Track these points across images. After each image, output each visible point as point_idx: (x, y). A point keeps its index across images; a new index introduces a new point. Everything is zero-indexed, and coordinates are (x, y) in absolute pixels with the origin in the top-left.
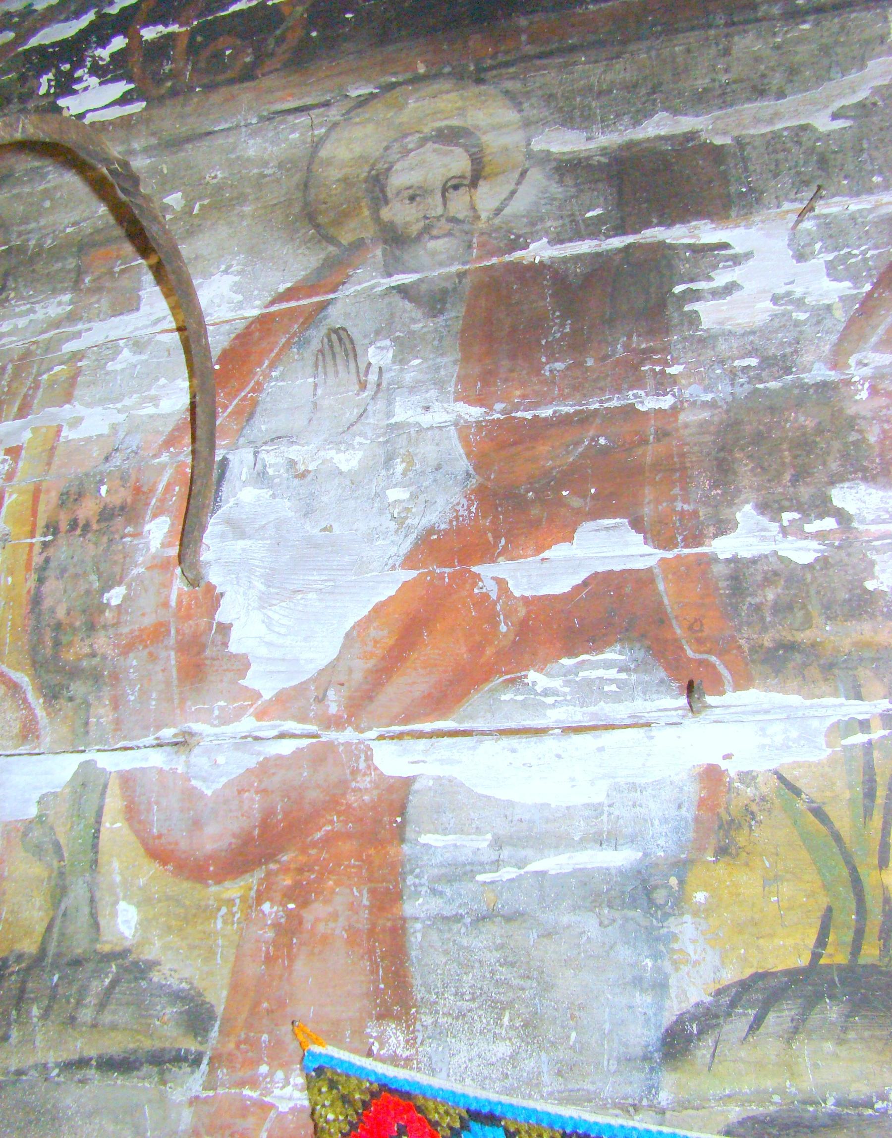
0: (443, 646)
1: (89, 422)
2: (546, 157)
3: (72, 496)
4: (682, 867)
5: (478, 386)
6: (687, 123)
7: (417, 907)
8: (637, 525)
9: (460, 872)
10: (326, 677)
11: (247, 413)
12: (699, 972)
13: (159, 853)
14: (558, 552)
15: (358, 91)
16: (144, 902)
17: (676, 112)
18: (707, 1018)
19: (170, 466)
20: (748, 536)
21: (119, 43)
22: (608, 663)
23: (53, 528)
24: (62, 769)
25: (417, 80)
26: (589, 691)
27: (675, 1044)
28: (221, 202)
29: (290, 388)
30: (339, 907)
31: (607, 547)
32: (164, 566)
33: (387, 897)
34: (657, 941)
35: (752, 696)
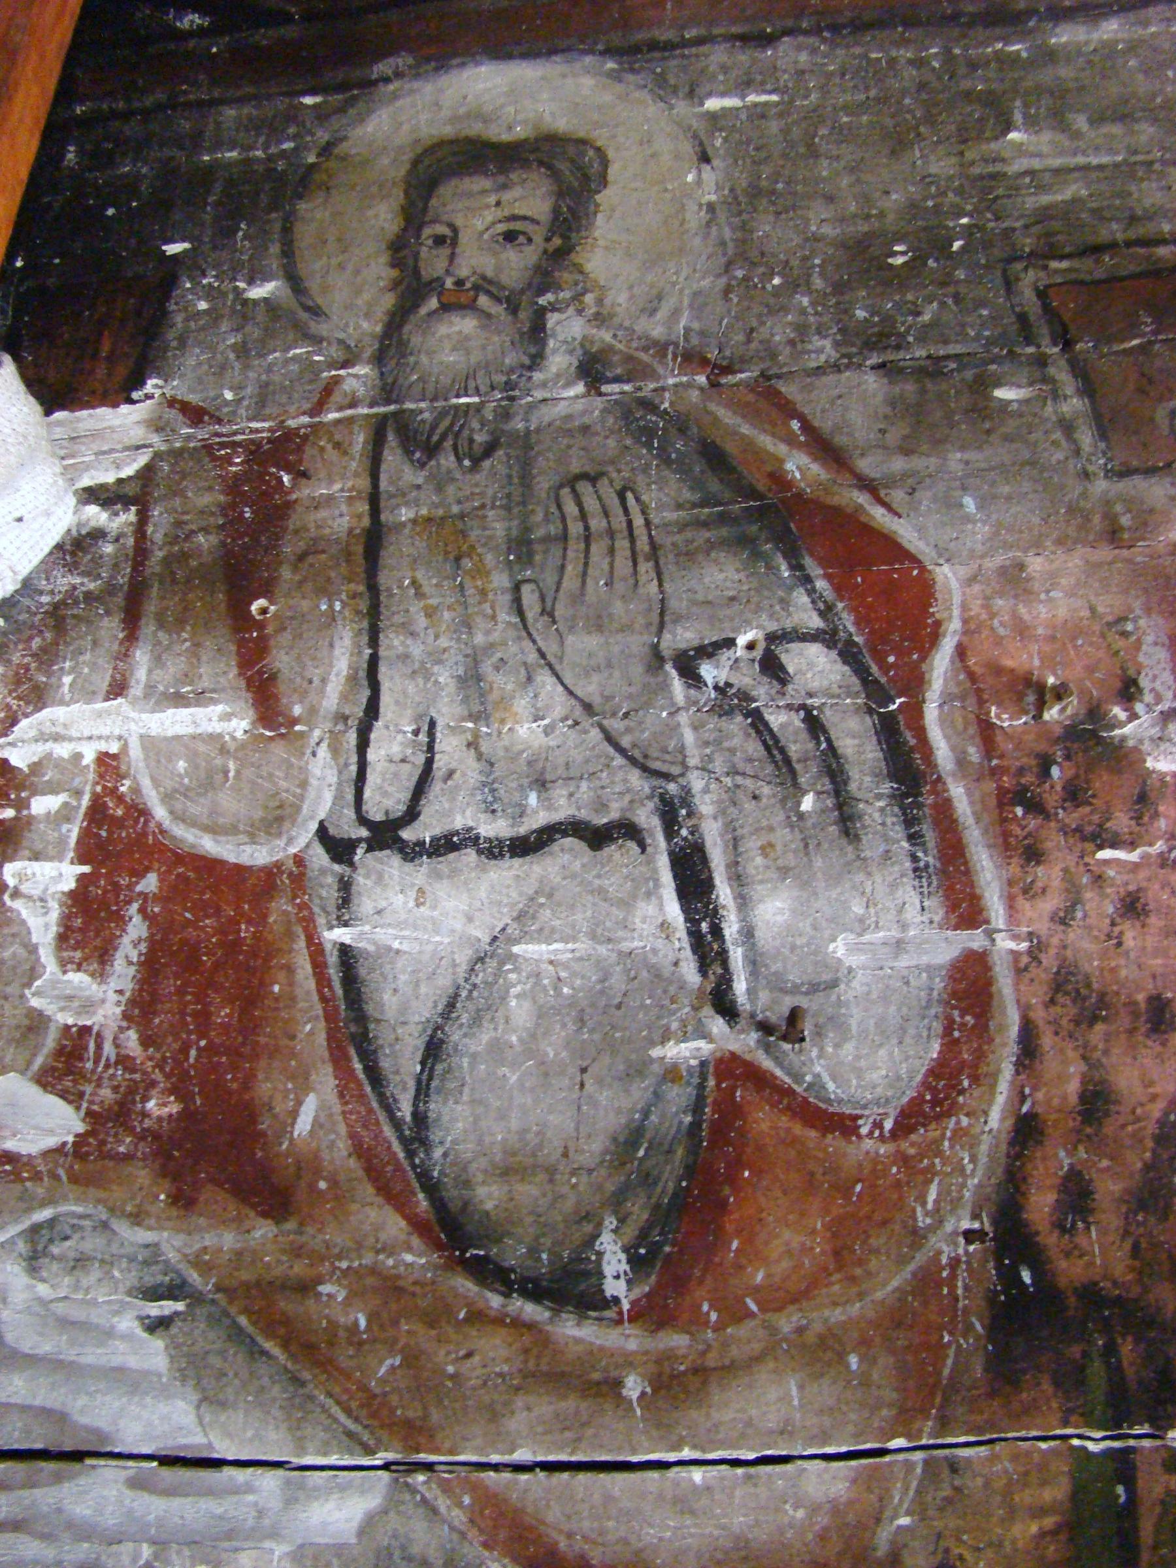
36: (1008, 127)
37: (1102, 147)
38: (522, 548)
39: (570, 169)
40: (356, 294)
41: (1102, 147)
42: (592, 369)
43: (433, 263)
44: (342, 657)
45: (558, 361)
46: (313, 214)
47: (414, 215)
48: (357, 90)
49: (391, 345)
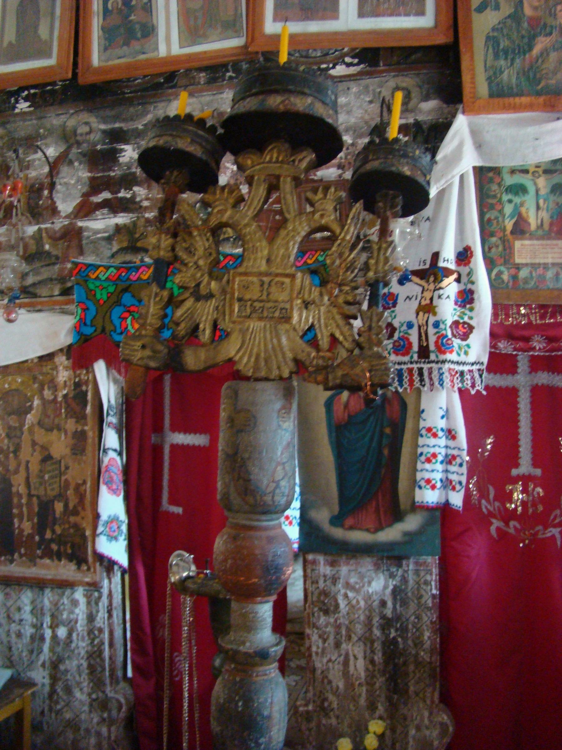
0: (86, 209)
1: (33, 174)
2: (100, 130)
3: (32, 186)
4: (114, 235)
5: (90, 171)
6: (122, 125)
7: (84, 242)
8: (110, 192)
9: (88, 237)
10: (71, 213)
11: (58, 173)
12: (115, 247)
13: (50, 237)
14: (100, 196)
15: (72, 111)
16: (49, 244)
17: (120, 122)
18: (117, 252)
19: (47, 181)
20: (122, 194)
21: (26, 93)
22: (105, 211)
23: (29, 192)
24: (36, 228)
25: (81, 111)
26: (103, 214)
27: (113, 256)
28: (50, 132)
29: (65, 170)
30: (74, 243)
31: (106, 195)
32: (47, 198)
33: (80, 241)
34: (111, 244)
35: (122, 214)
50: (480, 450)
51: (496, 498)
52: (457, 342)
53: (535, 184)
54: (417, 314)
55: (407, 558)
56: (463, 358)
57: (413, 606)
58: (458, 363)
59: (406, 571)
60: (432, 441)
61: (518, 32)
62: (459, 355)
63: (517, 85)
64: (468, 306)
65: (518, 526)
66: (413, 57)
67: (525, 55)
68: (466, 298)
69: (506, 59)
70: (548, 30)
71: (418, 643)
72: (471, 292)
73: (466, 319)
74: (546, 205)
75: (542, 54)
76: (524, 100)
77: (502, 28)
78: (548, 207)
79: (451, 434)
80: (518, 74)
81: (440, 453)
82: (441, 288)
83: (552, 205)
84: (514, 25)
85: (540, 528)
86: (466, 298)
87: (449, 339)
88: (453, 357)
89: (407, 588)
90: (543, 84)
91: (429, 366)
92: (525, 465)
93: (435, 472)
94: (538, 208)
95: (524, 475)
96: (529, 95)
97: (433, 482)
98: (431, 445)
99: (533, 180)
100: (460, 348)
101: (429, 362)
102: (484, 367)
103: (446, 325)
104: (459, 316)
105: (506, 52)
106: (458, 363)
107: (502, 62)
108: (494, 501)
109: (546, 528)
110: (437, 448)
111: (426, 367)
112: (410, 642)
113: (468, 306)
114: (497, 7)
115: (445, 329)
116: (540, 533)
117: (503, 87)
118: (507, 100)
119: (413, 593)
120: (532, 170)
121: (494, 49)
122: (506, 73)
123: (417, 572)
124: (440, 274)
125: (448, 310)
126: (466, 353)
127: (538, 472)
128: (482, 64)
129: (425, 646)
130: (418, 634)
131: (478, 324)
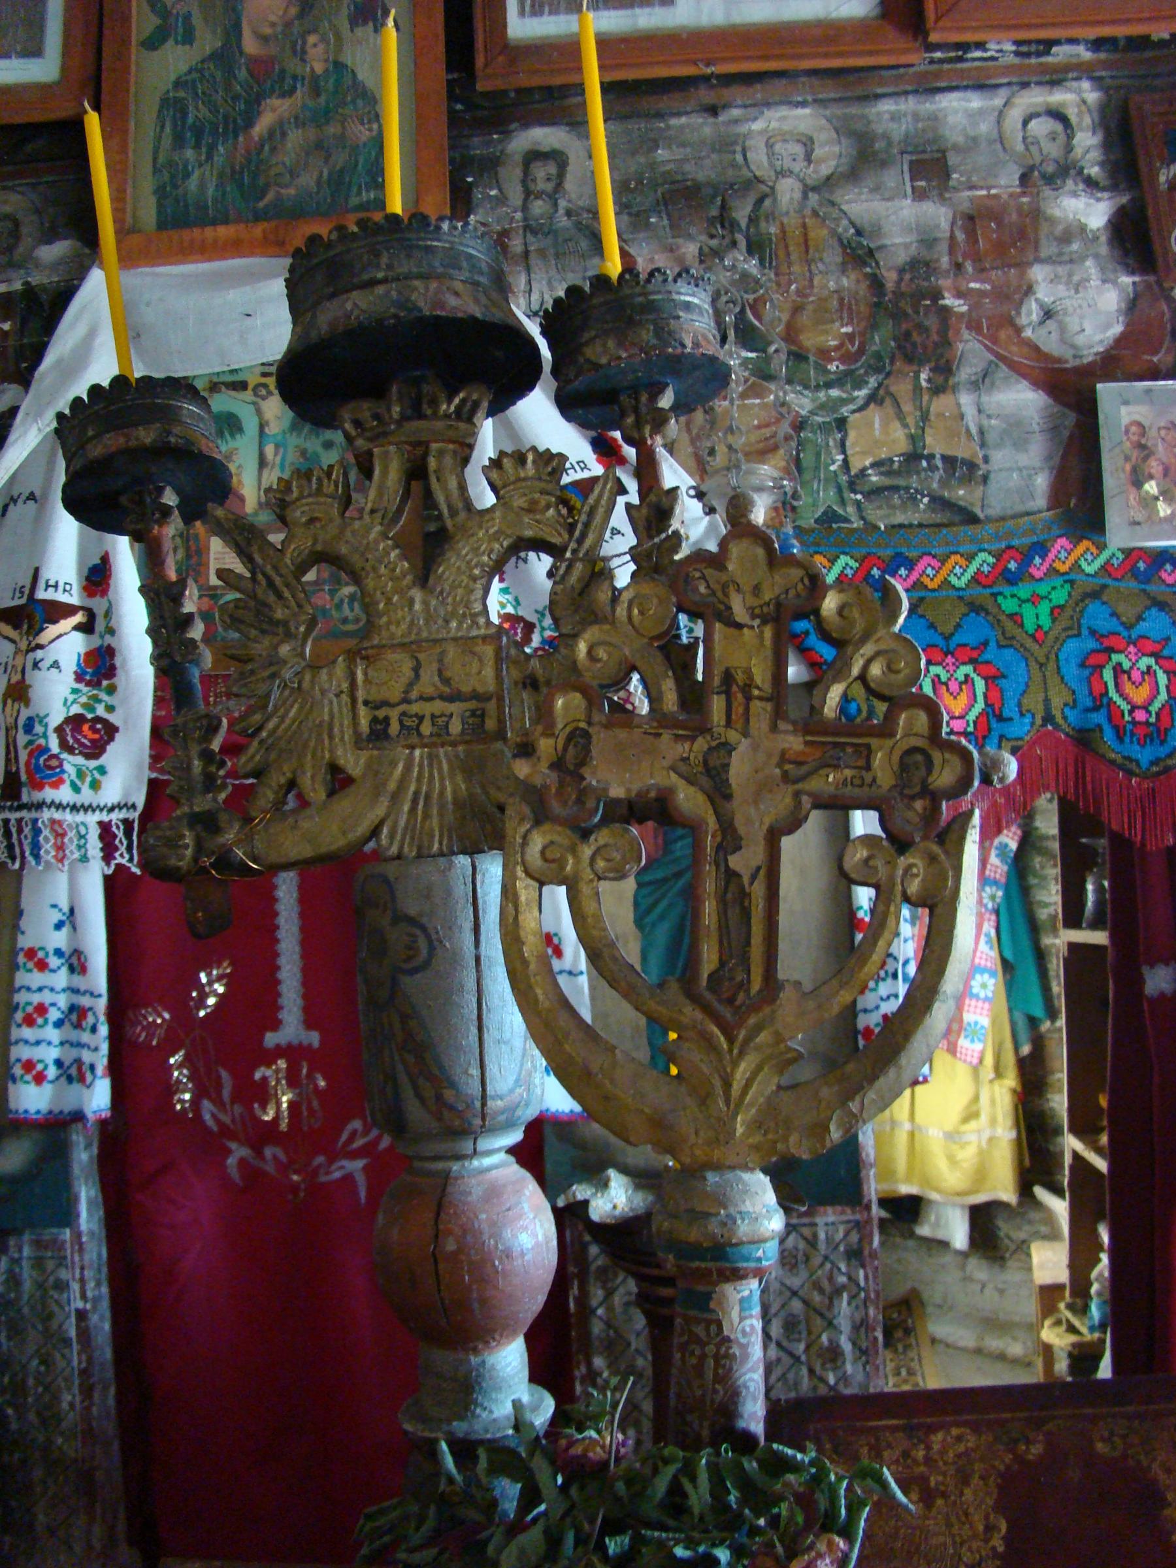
36: (657, 147)
37: (679, 153)
38: (557, 256)
39: (558, 158)
40: (515, 195)
41: (679, 153)
42: (569, 213)
43: (532, 187)
44: (523, 279)
45: (561, 211)
46: (502, 172)
47: (526, 172)
48: (506, 134)
49: (525, 208)
50: (194, 994)
51: (235, 1099)
52: (72, 763)
53: (259, 412)
54: (5, 704)
55: (18, 1232)
56: (87, 796)
57: (33, 1337)
58: (74, 808)
59: (17, 1261)
60: (36, 978)
61: (228, 87)
62: (76, 789)
63: (215, 200)
64: (105, 683)
65: (282, 1156)
66: (29, 148)
67: (236, 137)
68: (101, 667)
69: (197, 146)
70: (289, 81)
71: (49, 1417)
72: (110, 652)
73: (100, 711)
74: (278, 459)
75: (271, 134)
76: (222, 231)
77: (194, 81)
78: (283, 459)
79: (77, 963)
80: (221, 176)
81: (54, 1005)
82: (41, 647)
83: (292, 457)
84: (219, 75)
85: (320, 1159)
86: (101, 667)
87: (55, 756)
88: (64, 794)
89: (19, 1298)
90: (270, 196)
91: (18, 815)
92: (291, 1028)
93: (45, 1045)
94: (262, 463)
95: (290, 1046)
96: (238, 221)
97: (40, 1067)
98: (34, 987)
99: (254, 403)
100: (81, 774)
101: (21, 807)
102: (135, 815)
103: (46, 726)
104: (85, 706)
105: (198, 132)
106: (74, 808)
107: (189, 153)
108: (233, 1102)
109: (331, 1160)
110: (46, 991)
111: (13, 816)
112: (32, 1416)
113: (105, 683)
114: (188, 38)
115: (45, 736)
116: (322, 1171)
117: (186, 206)
118: (186, 235)
119: (32, 1308)
120: (253, 380)
121: (175, 126)
122: (195, 176)
123: (38, 1263)
124: (38, 617)
125: (57, 693)
126: (95, 786)
127: (314, 1038)
128: (150, 158)
129: (64, 1425)
130: (47, 1398)
131: (126, 722)
